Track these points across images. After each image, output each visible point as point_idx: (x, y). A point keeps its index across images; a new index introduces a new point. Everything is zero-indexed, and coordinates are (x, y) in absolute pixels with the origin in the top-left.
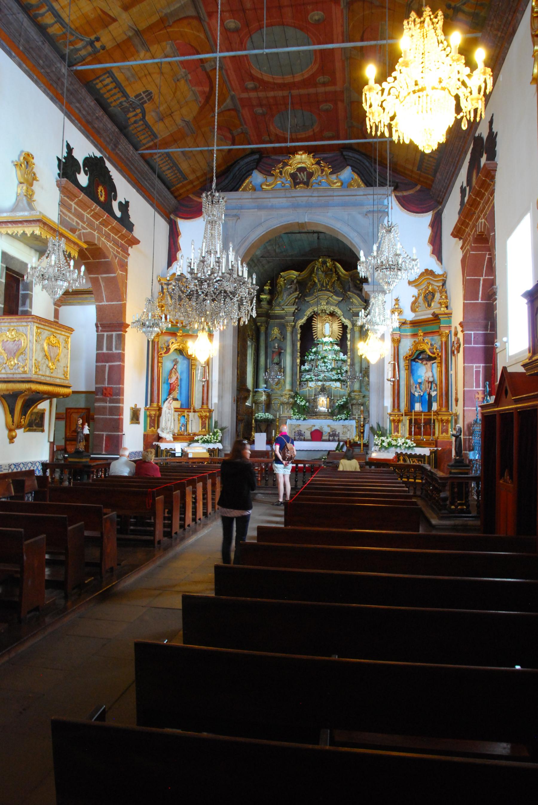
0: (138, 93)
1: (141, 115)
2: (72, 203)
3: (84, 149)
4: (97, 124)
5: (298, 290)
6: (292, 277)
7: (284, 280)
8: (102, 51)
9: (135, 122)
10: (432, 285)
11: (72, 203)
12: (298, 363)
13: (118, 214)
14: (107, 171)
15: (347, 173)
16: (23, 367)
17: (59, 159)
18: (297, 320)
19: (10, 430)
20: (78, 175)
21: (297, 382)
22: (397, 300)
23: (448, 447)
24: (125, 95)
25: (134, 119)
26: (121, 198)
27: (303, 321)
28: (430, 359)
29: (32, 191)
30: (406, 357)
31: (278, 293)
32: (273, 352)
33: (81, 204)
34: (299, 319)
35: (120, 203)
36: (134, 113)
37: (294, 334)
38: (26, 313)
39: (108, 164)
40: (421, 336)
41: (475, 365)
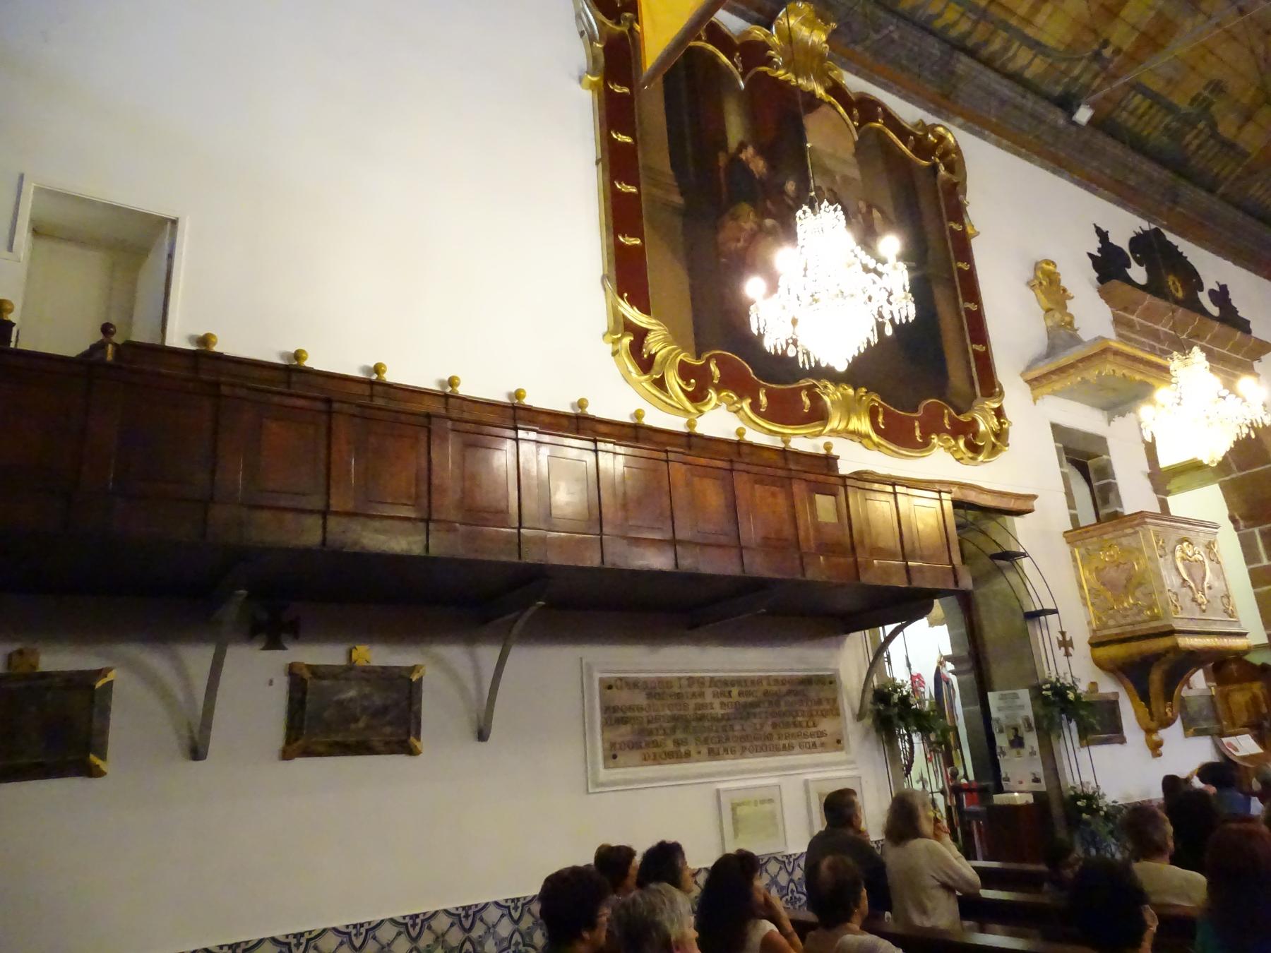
0: (1194, 93)
1: (1207, 130)
2: (1134, 317)
3: (1124, 226)
4: (1132, 181)
8: (1117, 59)
9: (1200, 147)
11: (1134, 317)
13: (1215, 311)
14: (1172, 249)
16: (1150, 608)
17: (1090, 255)
19: (1149, 732)
20: (1128, 271)
24: (1170, 108)
25: (1196, 142)
26: (1210, 283)
29: (1071, 316)
33: (1149, 314)
35: (1212, 292)
36: (1195, 132)
38: (1116, 516)
39: (1171, 237)
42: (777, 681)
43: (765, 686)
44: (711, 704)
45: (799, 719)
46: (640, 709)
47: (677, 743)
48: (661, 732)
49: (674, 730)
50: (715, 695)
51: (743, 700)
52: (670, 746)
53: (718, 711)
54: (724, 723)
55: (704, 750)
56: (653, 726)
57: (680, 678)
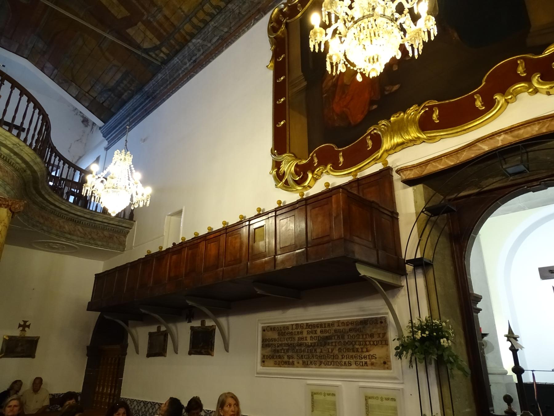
42: (343, 323)
43: (336, 327)
44: (306, 337)
45: (357, 347)
46: (275, 340)
47: (289, 357)
48: (283, 351)
49: (288, 350)
50: (308, 333)
51: (322, 335)
52: (286, 359)
53: (309, 341)
54: (311, 348)
55: (301, 362)
56: (280, 348)
57: (292, 325)
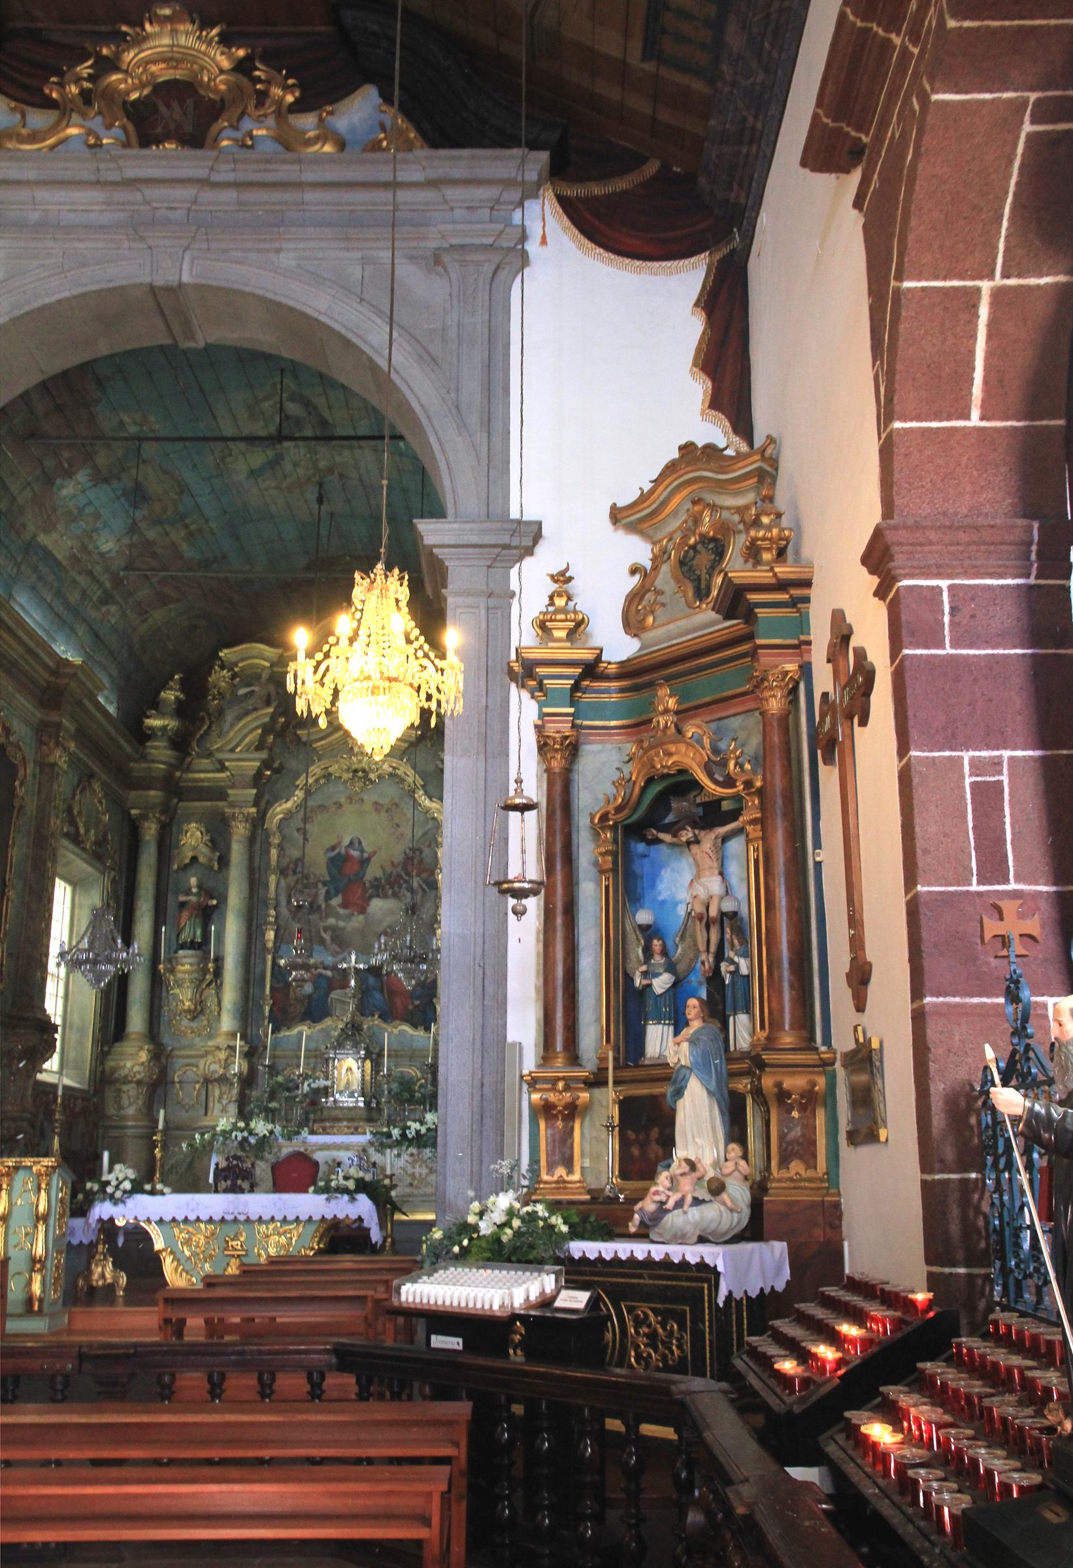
5: (274, 704)
6: (257, 666)
7: (233, 677)
10: (714, 508)
12: (270, 945)
15: (360, 110)
18: (270, 804)
21: (261, 1008)
22: (562, 578)
23: (819, 1234)
27: (289, 804)
28: (713, 815)
30: (604, 817)
31: (209, 714)
32: (183, 905)
34: (276, 799)
37: (258, 846)
40: (666, 711)
41: (967, 756)
